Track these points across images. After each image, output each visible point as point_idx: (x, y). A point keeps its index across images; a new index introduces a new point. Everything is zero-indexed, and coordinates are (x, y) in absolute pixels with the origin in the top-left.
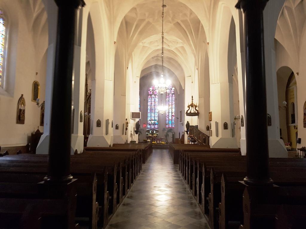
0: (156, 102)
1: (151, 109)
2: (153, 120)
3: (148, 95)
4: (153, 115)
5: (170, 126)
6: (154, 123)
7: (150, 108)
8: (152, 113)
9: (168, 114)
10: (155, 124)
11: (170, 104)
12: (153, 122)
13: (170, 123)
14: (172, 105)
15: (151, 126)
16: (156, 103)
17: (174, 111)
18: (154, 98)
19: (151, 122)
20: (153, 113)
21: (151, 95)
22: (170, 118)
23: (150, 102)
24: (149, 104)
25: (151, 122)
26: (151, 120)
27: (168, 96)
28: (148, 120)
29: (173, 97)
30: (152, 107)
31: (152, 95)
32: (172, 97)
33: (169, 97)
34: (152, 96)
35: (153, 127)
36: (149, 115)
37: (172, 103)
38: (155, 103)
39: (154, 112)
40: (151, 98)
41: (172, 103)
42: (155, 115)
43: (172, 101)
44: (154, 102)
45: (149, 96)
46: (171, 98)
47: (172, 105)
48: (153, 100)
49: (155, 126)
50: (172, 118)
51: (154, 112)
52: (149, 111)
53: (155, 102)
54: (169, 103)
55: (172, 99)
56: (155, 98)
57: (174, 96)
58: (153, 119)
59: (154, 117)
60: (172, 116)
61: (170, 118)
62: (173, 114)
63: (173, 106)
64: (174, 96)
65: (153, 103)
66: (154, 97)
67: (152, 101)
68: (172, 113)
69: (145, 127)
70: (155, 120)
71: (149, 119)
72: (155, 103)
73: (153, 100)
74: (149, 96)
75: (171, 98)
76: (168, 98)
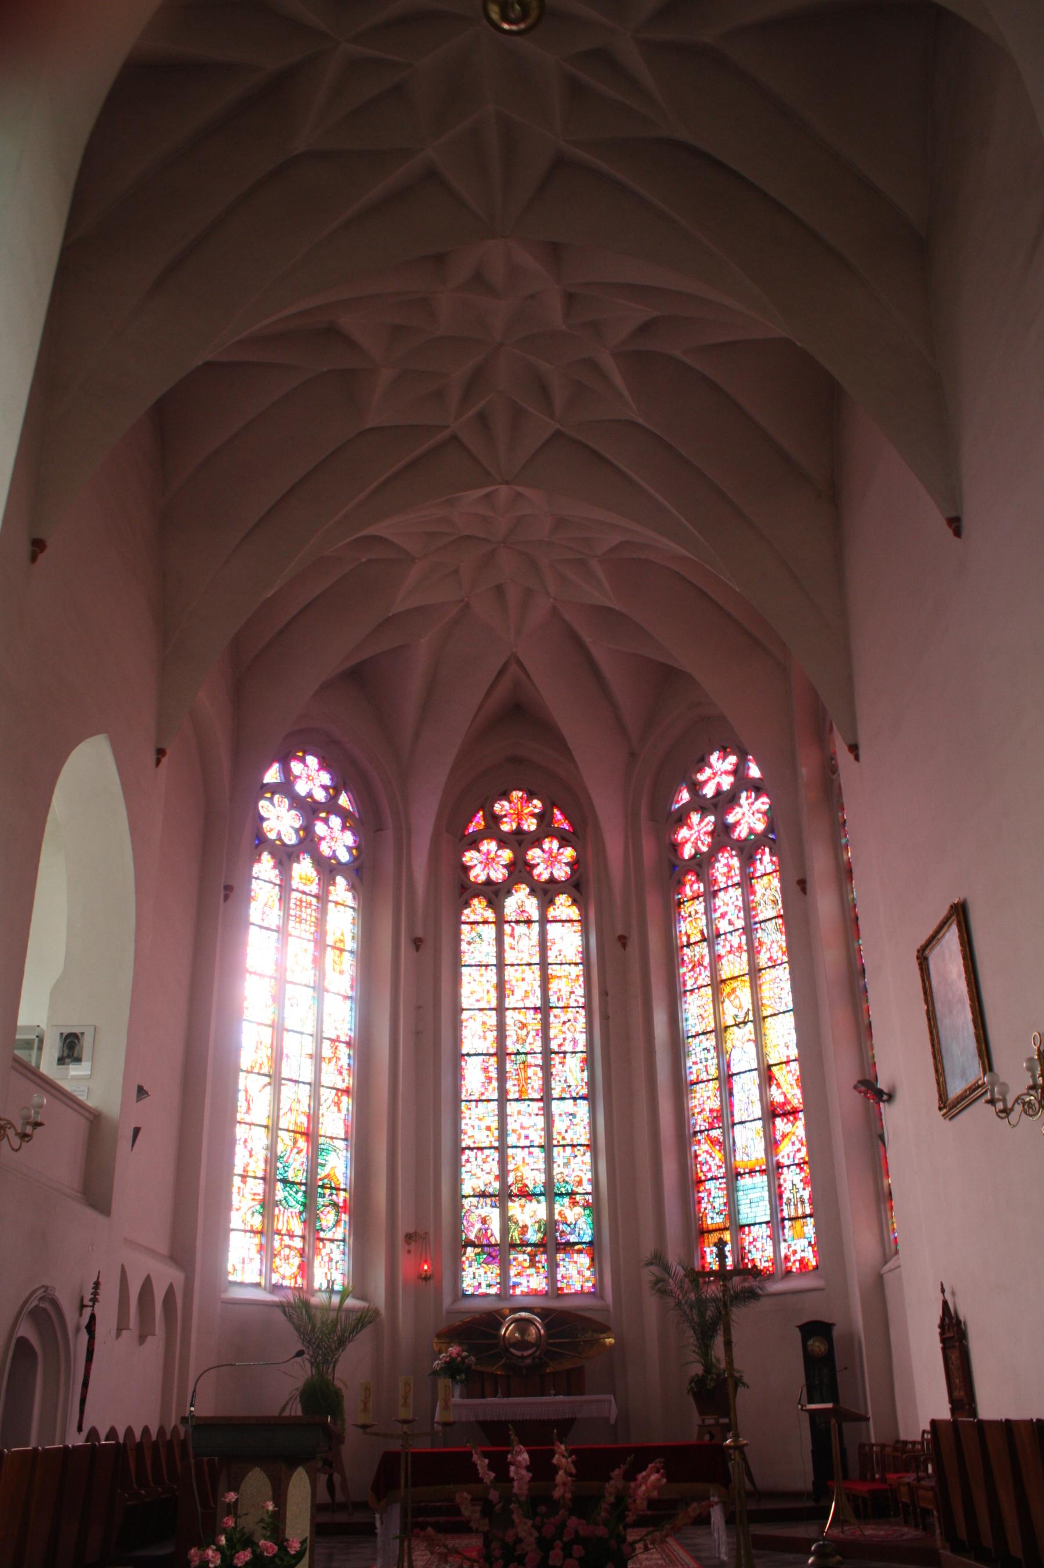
0: (552, 970)
1: (501, 1054)
2: (526, 1194)
3: (466, 891)
4: (526, 1120)
5: (761, 1252)
6: (550, 1226)
7: (489, 1044)
8: (512, 1108)
9: (715, 1104)
10: (552, 1244)
11: (734, 965)
12: (529, 1215)
13: (754, 1201)
14: (755, 972)
15: (504, 1275)
16: (554, 986)
17: (794, 1053)
18: (529, 922)
19: (506, 1220)
20: (536, 1106)
21: (495, 894)
22: (750, 1144)
23: (492, 975)
24: (475, 988)
25: (506, 1220)
26: (504, 1196)
27: (701, 887)
28: (466, 1189)
29: (759, 886)
30: (511, 1032)
31: (509, 893)
32: (747, 883)
33: (711, 894)
34: (511, 905)
35: (537, 1282)
36: (477, 1124)
37: (753, 951)
38: (545, 980)
39: (547, 1087)
40: (500, 922)
41: (753, 951)
42: (559, 1125)
43: (749, 930)
44: (533, 976)
45: (478, 909)
46: (729, 901)
47: (755, 972)
48: (523, 944)
49: (553, 1266)
50: (772, 1144)
51: (547, 1087)
52: (474, 1077)
53: (544, 964)
54: (716, 959)
55: (748, 909)
56: (544, 921)
57: (766, 862)
58: (534, 1179)
59: (548, 1147)
60: (772, 1112)
61: (750, 1144)
62: (788, 1088)
63: (766, 992)
64: (766, 862)
65: (524, 986)
66: (532, 907)
67: (510, 957)
68: (767, 1076)
69: (426, 1279)
70: (550, 1192)
71: (477, 1174)
72: (545, 980)
73: (523, 944)
74: (478, 909)
75: (729, 901)
76: (699, 906)
